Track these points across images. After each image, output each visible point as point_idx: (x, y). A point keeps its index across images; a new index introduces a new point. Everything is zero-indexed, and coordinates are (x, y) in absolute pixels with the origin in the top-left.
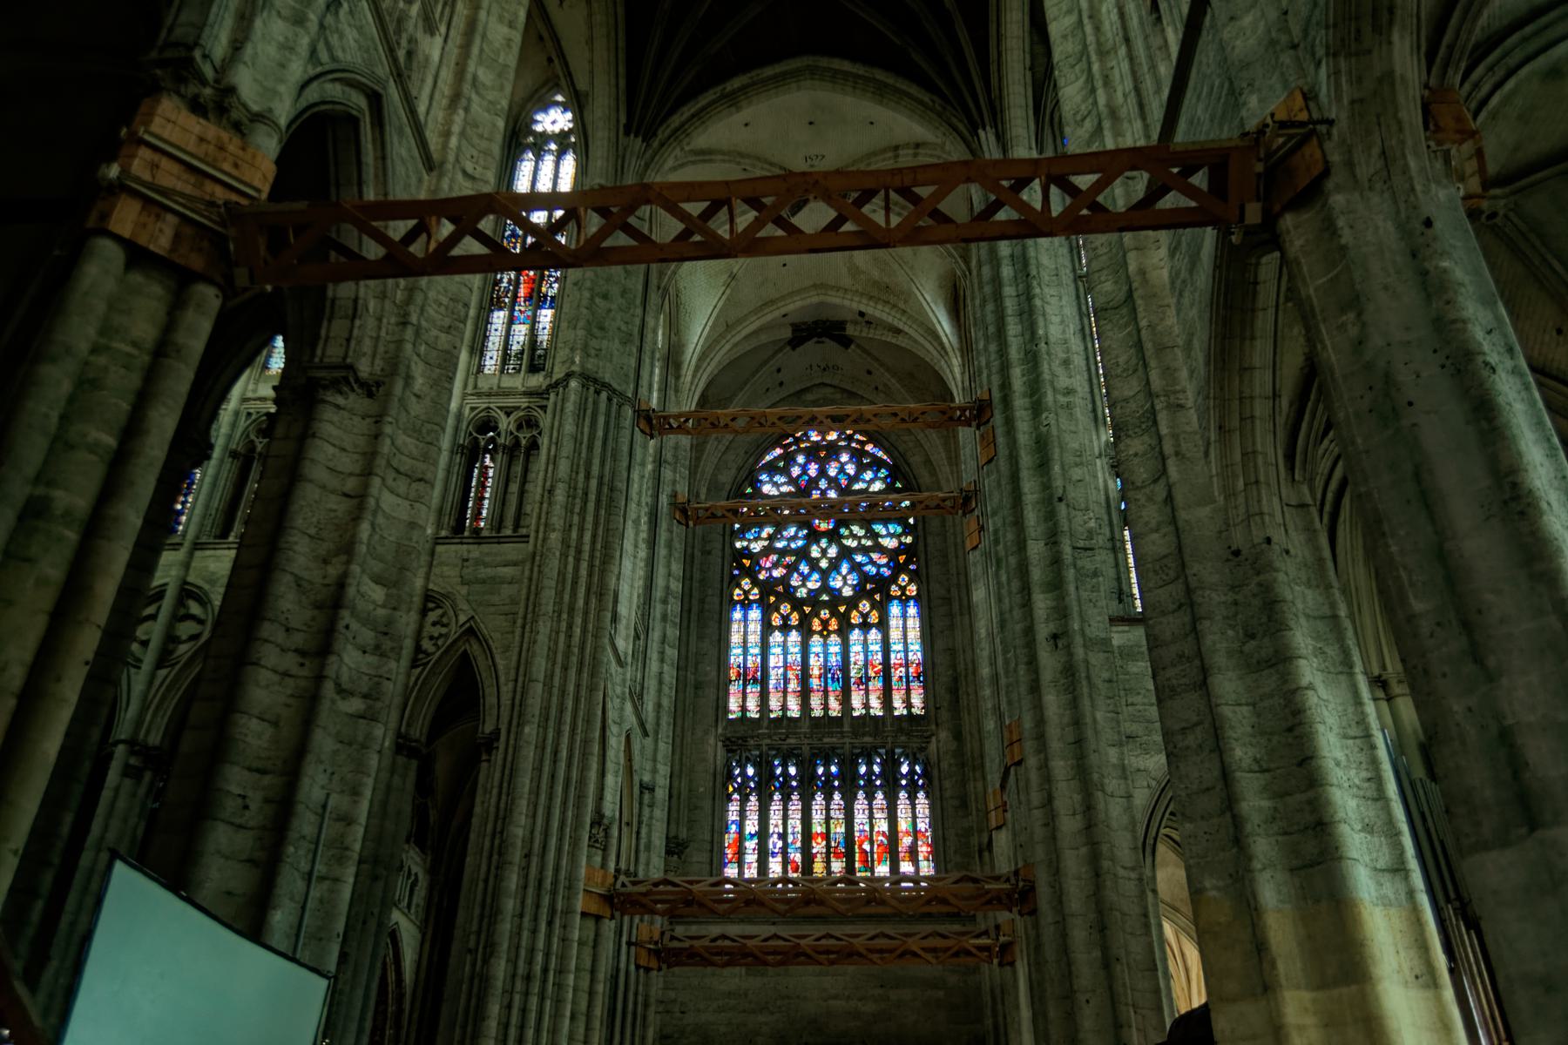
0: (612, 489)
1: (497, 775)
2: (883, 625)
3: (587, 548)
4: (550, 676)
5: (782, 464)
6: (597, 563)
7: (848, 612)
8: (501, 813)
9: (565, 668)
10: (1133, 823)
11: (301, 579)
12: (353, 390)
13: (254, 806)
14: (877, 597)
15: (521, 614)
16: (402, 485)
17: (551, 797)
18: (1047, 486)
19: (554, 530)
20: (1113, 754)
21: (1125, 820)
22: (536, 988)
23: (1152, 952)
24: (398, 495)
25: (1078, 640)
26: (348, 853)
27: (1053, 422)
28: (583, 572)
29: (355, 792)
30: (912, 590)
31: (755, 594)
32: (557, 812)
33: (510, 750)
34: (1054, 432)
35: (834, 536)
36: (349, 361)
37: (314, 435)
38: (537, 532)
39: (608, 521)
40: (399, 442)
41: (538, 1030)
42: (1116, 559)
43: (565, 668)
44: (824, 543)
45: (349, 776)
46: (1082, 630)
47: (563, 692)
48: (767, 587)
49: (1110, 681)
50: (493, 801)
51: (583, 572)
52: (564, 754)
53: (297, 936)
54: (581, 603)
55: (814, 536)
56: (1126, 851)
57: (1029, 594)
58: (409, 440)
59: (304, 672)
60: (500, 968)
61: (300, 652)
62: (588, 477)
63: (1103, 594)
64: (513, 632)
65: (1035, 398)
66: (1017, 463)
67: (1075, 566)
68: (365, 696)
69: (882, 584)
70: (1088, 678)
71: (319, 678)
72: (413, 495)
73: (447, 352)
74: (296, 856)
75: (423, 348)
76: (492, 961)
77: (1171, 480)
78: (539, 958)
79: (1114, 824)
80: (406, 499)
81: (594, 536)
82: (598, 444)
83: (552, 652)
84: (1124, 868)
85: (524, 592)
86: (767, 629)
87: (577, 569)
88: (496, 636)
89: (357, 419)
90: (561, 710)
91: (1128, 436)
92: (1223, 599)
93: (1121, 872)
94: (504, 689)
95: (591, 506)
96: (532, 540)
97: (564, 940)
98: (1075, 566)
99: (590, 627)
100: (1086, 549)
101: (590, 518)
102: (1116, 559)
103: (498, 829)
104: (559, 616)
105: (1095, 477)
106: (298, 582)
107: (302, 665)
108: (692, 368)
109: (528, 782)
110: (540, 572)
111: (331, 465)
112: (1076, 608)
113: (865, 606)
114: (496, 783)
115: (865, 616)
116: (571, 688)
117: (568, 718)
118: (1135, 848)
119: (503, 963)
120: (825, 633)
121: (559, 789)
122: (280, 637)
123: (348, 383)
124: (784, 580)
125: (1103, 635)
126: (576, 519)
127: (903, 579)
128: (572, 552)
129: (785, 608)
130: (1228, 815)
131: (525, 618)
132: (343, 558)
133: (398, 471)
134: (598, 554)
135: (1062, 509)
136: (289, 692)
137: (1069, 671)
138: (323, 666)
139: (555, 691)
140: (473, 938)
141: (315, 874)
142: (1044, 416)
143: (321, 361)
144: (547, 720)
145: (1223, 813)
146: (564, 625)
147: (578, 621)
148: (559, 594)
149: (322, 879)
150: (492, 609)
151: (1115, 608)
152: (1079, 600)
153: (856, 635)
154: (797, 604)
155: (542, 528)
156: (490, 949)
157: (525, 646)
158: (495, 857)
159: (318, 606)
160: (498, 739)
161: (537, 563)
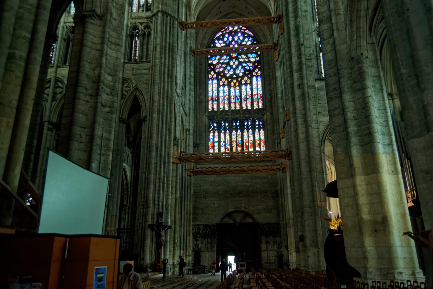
0: (173, 46)
1: (147, 128)
2: (251, 84)
3: (167, 64)
4: (159, 101)
5: (221, 37)
6: (170, 68)
8: (149, 138)
9: (163, 98)
10: (319, 135)
11: (88, 75)
12: (96, 18)
13: (83, 137)
14: (249, 76)
15: (150, 83)
16: (113, 47)
17: (162, 133)
18: (298, 41)
19: (157, 59)
20: (314, 117)
21: (317, 135)
22: (162, 181)
23: (322, 168)
24: (112, 50)
25: (306, 86)
26: (109, 148)
27: (301, 21)
28: (166, 71)
29: (110, 133)
30: (259, 73)
31: (215, 76)
32: (164, 137)
33: (150, 121)
34: (301, 24)
35: (237, 58)
36: (93, 9)
37: (86, 32)
38: (153, 59)
39: (172, 56)
40: (111, 34)
41: (163, 191)
42: (318, 62)
43: (163, 98)
44: (234, 60)
45: (108, 128)
46: (307, 83)
47: (163, 105)
48: (218, 74)
49: (314, 97)
50: (147, 134)
51: (166, 71)
52: (165, 121)
53: (99, 169)
54: (166, 80)
55: (231, 58)
56: (317, 143)
57: (292, 73)
58: (113, 33)
59: (92, 101)
60: (152, 177)
61: (90, 95)
62: (166, 43)
63: (313, 72)
64: (148, 89)
65: (295, 14)
66: (290, 34)
67: (306, 64)
68: (110, 107)
69: (251, 72)
70: (308, 96)
71: (97, 102)
72: (116, 49)
73: (122, 5)
74: (96, 150)
75: (115, 4)
76: (150, 175)
77: (335, 37)
78: (162, 174)
79: (314, 136)
80: (115, 50)
81: (169, 60)
82: (168, 33)
83: (159, 94)
84: (316, 147)
85: (150, 77)
86: (219, 86)
87: (164, 70)
88: (144, 90)
89: (98, 27)
90: (163, 110)
91: (323, 24)
92: (348, 72)
93: (315, 148)
94: (147, 104)
95: (167, 51)
96: (151, 62)
97: (168, 169)
98: (306, 64)
99: (169, 86)
100: (309, 59)
101: (167, 55)
102: (318, 62)
103: (149, 142)
104: (161, 83)
105: (313, 37)
106: (87, 75)
107: (91, 99)
108: (194, 8)
109: (155, 129)
110: (154, 71)
111: (92, 41)
112: (305, 77)
113: (246, 78)
114: (147, 130)
115: (246, 81)
116: (165, 103)
117: (165, 112)
118: (319, 142)
119: (153, 175)
120: (235, 86)
121: (164, 131)
122: (84, 91)
123: (94, 16)
124: (223, 72)
125: (313, 84)
126: (163, 55)
128: (163, 65)
129: (224, 80)
130: (345, 132)
131: (151, 84)
132: (99, 68)
133: (111, 43)
134: (170, 66)
135: (303, 48)
136: (89, 106)
137: (303, 95)
138: (97, 99)
139: (161, 104)
140: (145, 169)
141: (102, 154)
142: (298, 19)
143: (86, 8)
144: (159, 112)
145: (344, 131)
146: (162, 86)
147: (166, 85)
148: (160, 77)
149: (104, 155)
150: (142, 82)
151: (317, 76)
152: (306, 75)
153: (243, 87)
154: (227, 79)
155: (154, 59)
156: (149, 172)
157: (152, 93)
158: (149, 149)
159: (93, 82)
160: (146, 118)
161: (153, 69)
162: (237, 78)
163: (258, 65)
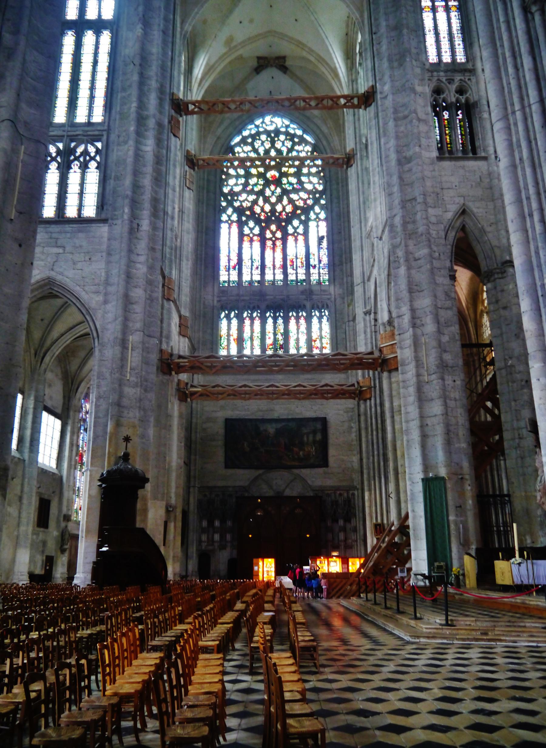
2: (306, 234)
7: (286, 226)
14: (303, 218)
30: (323, 215)
31: (235, 217)
35: (277, 182)
44: (273, 187)
48: (240, 211)
55: (267, 183)
69: (307, 210)
86: (241, 236)
108: (198, 80)
113: (296, 223)
115: (295, 229)
124: (251, 209)
127: (317, 209)
129: (251, 224)
153: (291, 239)
154: (258, 221)
162: (278, 221)
163: (321, 197)
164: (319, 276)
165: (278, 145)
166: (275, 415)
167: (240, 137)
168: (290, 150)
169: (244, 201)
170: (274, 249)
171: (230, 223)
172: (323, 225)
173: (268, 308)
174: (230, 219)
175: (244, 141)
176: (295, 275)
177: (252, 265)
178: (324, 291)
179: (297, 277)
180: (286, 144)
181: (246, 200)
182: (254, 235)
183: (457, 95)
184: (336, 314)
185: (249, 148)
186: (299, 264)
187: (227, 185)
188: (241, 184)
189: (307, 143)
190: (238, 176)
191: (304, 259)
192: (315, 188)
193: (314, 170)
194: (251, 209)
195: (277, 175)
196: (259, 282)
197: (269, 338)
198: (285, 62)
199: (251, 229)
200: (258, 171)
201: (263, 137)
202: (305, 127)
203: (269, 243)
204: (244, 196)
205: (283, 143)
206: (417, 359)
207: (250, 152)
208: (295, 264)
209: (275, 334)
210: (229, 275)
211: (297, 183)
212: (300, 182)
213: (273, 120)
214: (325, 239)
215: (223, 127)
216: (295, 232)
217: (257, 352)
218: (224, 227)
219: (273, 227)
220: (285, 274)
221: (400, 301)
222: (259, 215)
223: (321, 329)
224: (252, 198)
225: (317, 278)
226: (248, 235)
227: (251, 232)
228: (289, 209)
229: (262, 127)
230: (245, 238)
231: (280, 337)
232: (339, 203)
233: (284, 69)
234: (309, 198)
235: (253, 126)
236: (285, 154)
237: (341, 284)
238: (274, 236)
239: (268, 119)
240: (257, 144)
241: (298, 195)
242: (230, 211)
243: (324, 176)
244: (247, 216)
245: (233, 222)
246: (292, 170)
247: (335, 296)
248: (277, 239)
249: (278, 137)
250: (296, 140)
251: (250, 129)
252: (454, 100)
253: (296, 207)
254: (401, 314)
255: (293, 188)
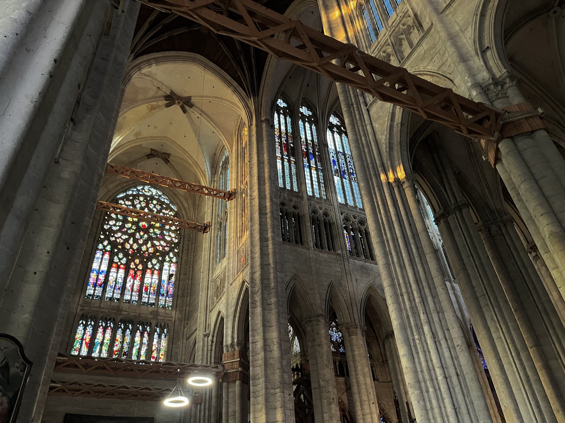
2: (161, 270)
7: (147, 262)
14: (160, 258)
30: (174, 260)
31: (108, 248)
35: (146, 231)
48: (114, 245)
55: (139, 229)
69: (164, 254)
86: (111, 263)
113: (154, 261)
124: (123, 244)
127: (171, 255)
129: (121, 255)
154: (126, 255)
162: (142, 257)
163: (175, 247)
164: (165, 302)
165: (151, 206)
166: (111, 413)
167: (125, 194)
168: (159, 212)
169: (118, 238)
170: (134, 277)
171: (104, 252)
172: (173, 268)
173: (122, 321)
174: (104, 249)
175: (126, 198)
176: (147, 299)
177: (115, 286)
178: (167, 314)
179: (148, 300)
180: (157, 207)
181: (120, 237)
182: (122, 264)
183: (293, 209)
184: (174, 333)
185: (130, 203)
186: (152, 291)
187: (108, 224)
188: (119, 226)
189: (172, 210)
190: (117, 220)
191: (156, 288)
192: (172, 240)
193: (173, 228)
194: (123, 244)
195: (147, 226)
196: (118, 299)
197: (117, 345)
198: (169, 157)
199: (120, 259)
200: (133, 220)
201: (141, 199)
202: (172, 199)
203: (132, 272)
204: (119, 234)
205: (155, 205)
206: (266, 376)
207: (130, 206)
208: (149, 290)
209: (122, 343)
210: (95, 290)
211: (159, 234)
212: (162, 234)
213: (151, 189)
214: (174, 276)
215: (114, 184)
216: (153, 267)
217: (104, 355)
218: (98, 255)
219: (137, 261)
220: (140, 296)
221: (254, 332)
222: (128, 250)
223: (159, 343)
224: (124, 237)
225: (164, 304)
226: (117, 263)
227: (120, 261)
228: (151, 250)
229: (142, 192)
230: (114, 265)
231: (126, 346)
232: (188, 253)
233: (167, 161)
234: (167, 246)
235: (135, 189)
236: (155, 212)
237: (181, 312)
238: (136, 268)
239: (146, 188)
240: (136, 202)
241: (160, 242)
242: (106, 243)
243: (179, 234)
244: (118, 249)
245: (106, 251)
246: (158, 225)
247: (175, 319)
248: (138, 270)
249: (152, 201)
250: (164, 206)
251: (133, 191)
252: (292, 211)
253: (157, 251)
254: (254, 341)
255: (157, 237)
